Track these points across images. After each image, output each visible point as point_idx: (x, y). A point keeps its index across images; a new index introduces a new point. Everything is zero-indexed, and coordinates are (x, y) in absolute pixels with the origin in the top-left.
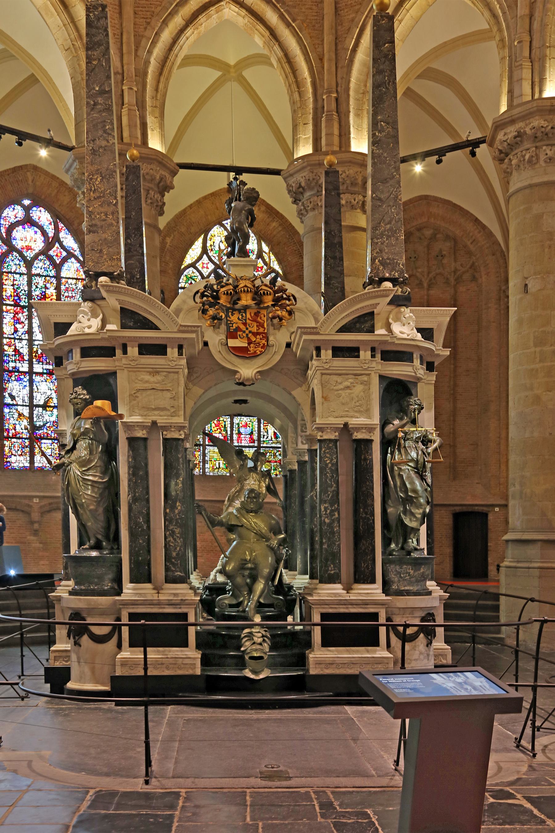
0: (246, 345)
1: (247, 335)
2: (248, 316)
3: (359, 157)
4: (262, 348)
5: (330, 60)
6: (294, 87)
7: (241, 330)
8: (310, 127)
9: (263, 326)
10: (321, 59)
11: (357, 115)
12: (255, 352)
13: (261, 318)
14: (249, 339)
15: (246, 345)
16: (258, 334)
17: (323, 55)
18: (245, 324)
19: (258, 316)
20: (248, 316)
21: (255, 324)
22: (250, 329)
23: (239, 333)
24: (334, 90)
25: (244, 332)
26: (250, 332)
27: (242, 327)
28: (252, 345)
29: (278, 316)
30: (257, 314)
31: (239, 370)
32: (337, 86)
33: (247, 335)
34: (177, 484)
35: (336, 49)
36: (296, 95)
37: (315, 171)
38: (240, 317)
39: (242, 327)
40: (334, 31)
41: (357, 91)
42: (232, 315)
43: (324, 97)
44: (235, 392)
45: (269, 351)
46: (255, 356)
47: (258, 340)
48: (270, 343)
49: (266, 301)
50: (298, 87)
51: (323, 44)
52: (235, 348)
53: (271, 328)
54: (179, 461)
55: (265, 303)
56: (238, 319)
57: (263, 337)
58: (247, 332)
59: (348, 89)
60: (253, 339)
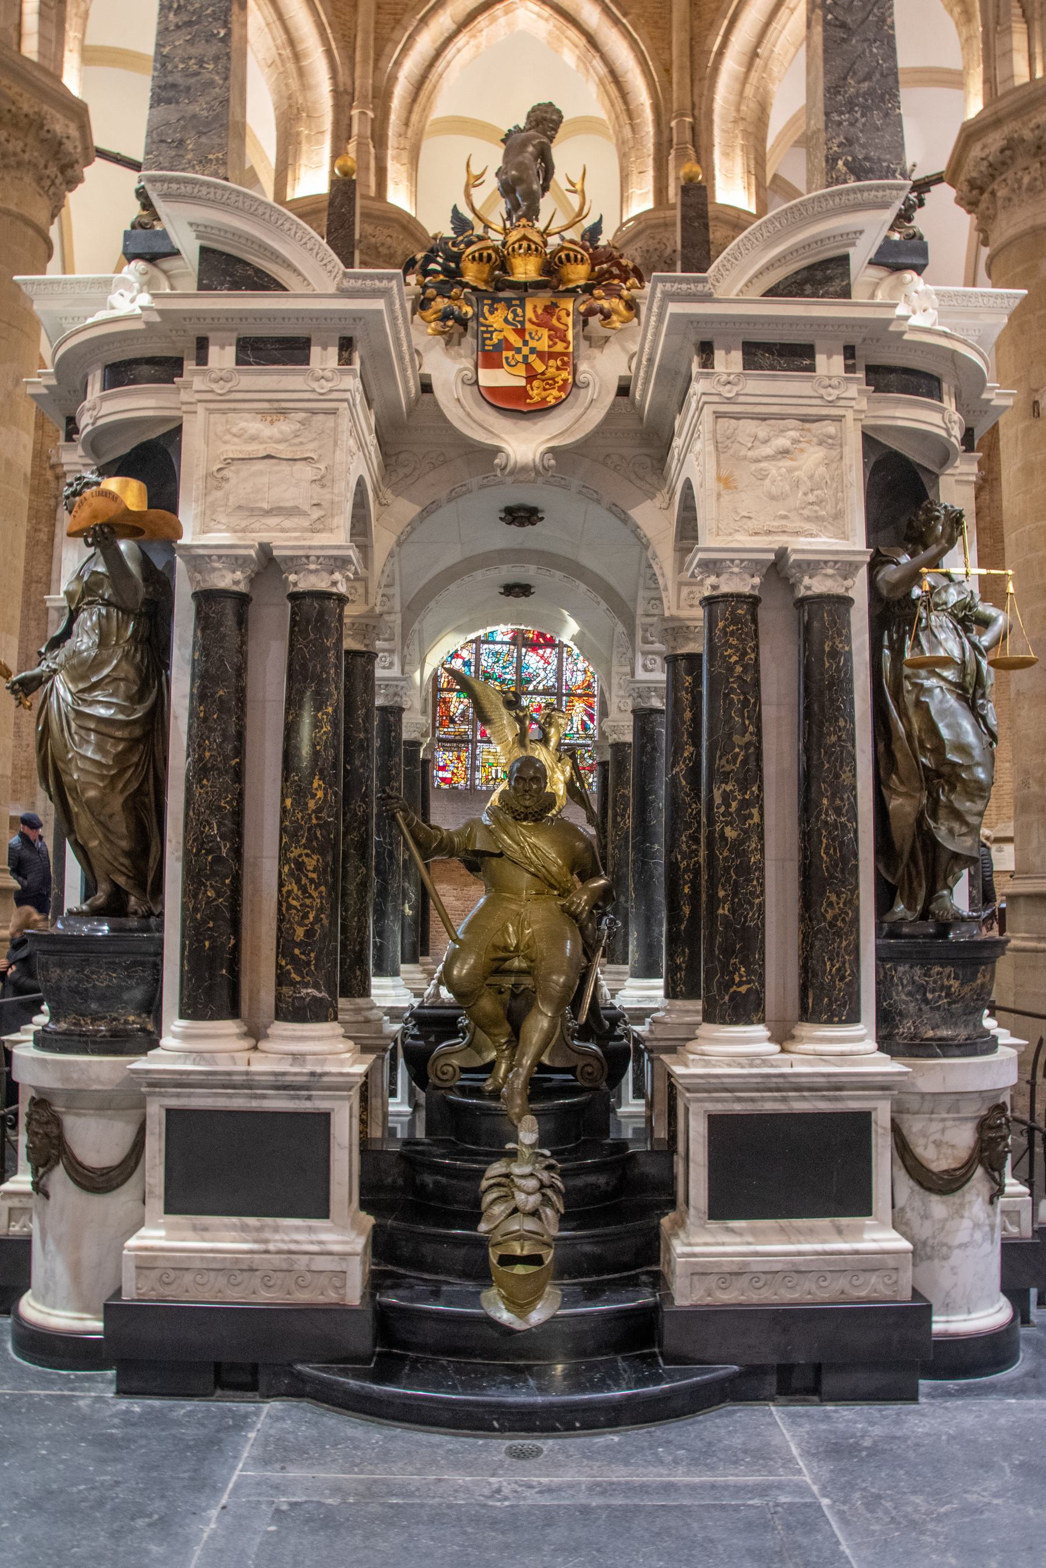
0: (522, 382)
1: (525, 357)
2: (530, 314)
3: (733, 213)
4: (560, 389)
5: (681, 68)
6: (624, 118)
7: (510, 347)
8: (650, 174)
9: (564, 339)
10: (668, 71)
11: (726, 154)
12: (544, 399)
13: (559, 319)
14: (529, 366)
15: (522, 382)
16: (552, 355)
17: (671, 64)
18: (521, 332)
19: (552, 315)
20: (530, 314)
21: (545, 333)
22: (532, 344)
23: (505, 354)
24: (689, 112)
25: (518, 351)
26: (533, 350)
27: (515, 340)
28: (536, 383)
29: (601, 311)
30: (550, 309)
31: (503, 445)
32: (693, 108)
33: (525, 357)
34: (316, 725)
35: (692, 55)
36: (627, 132)
37: (658, 237)
38: (510, 317)
39: (515, 340)
40: (687, 26)
41: (723, 119)
42: (491, 313)
43: (673, 124)
44: (503, 556)
45: (577, 399)
46: (544, 410)
47: (552, 371)
48: (581, 377)
49: (572, 277)
50: (631, 118)
51: (670, 48)
52: (493, 390)
53: (584, 344)
54: (326, 657)
55: (570, 281)
56: (506, 320)
57: (564, 363)
58: (525, 351)
59: (710, 111)
60: (539, 367)
